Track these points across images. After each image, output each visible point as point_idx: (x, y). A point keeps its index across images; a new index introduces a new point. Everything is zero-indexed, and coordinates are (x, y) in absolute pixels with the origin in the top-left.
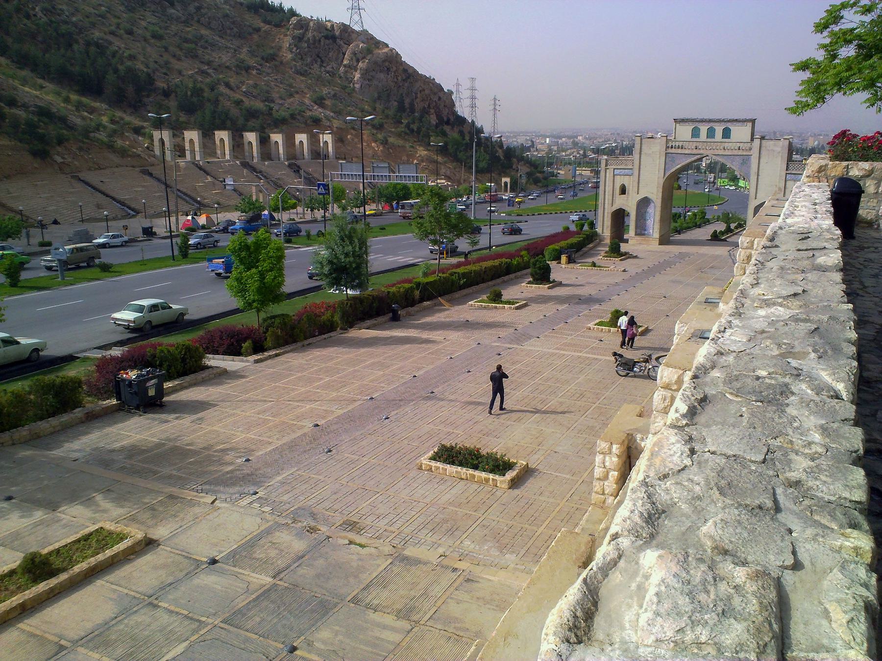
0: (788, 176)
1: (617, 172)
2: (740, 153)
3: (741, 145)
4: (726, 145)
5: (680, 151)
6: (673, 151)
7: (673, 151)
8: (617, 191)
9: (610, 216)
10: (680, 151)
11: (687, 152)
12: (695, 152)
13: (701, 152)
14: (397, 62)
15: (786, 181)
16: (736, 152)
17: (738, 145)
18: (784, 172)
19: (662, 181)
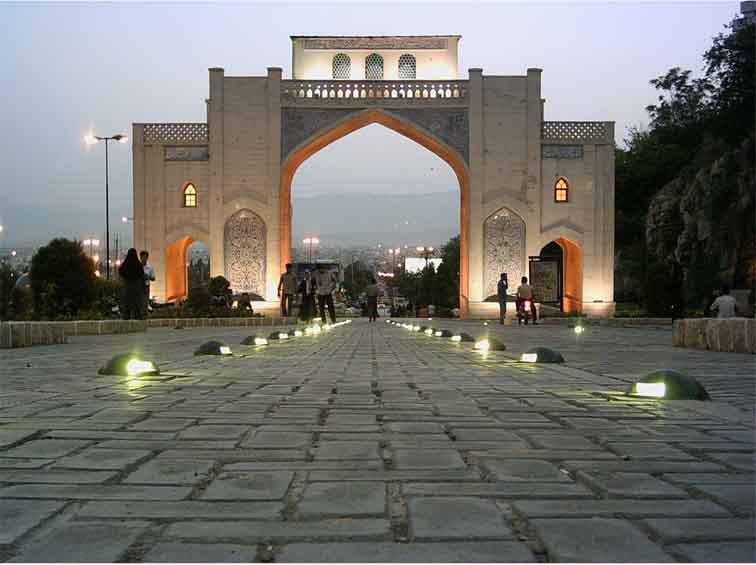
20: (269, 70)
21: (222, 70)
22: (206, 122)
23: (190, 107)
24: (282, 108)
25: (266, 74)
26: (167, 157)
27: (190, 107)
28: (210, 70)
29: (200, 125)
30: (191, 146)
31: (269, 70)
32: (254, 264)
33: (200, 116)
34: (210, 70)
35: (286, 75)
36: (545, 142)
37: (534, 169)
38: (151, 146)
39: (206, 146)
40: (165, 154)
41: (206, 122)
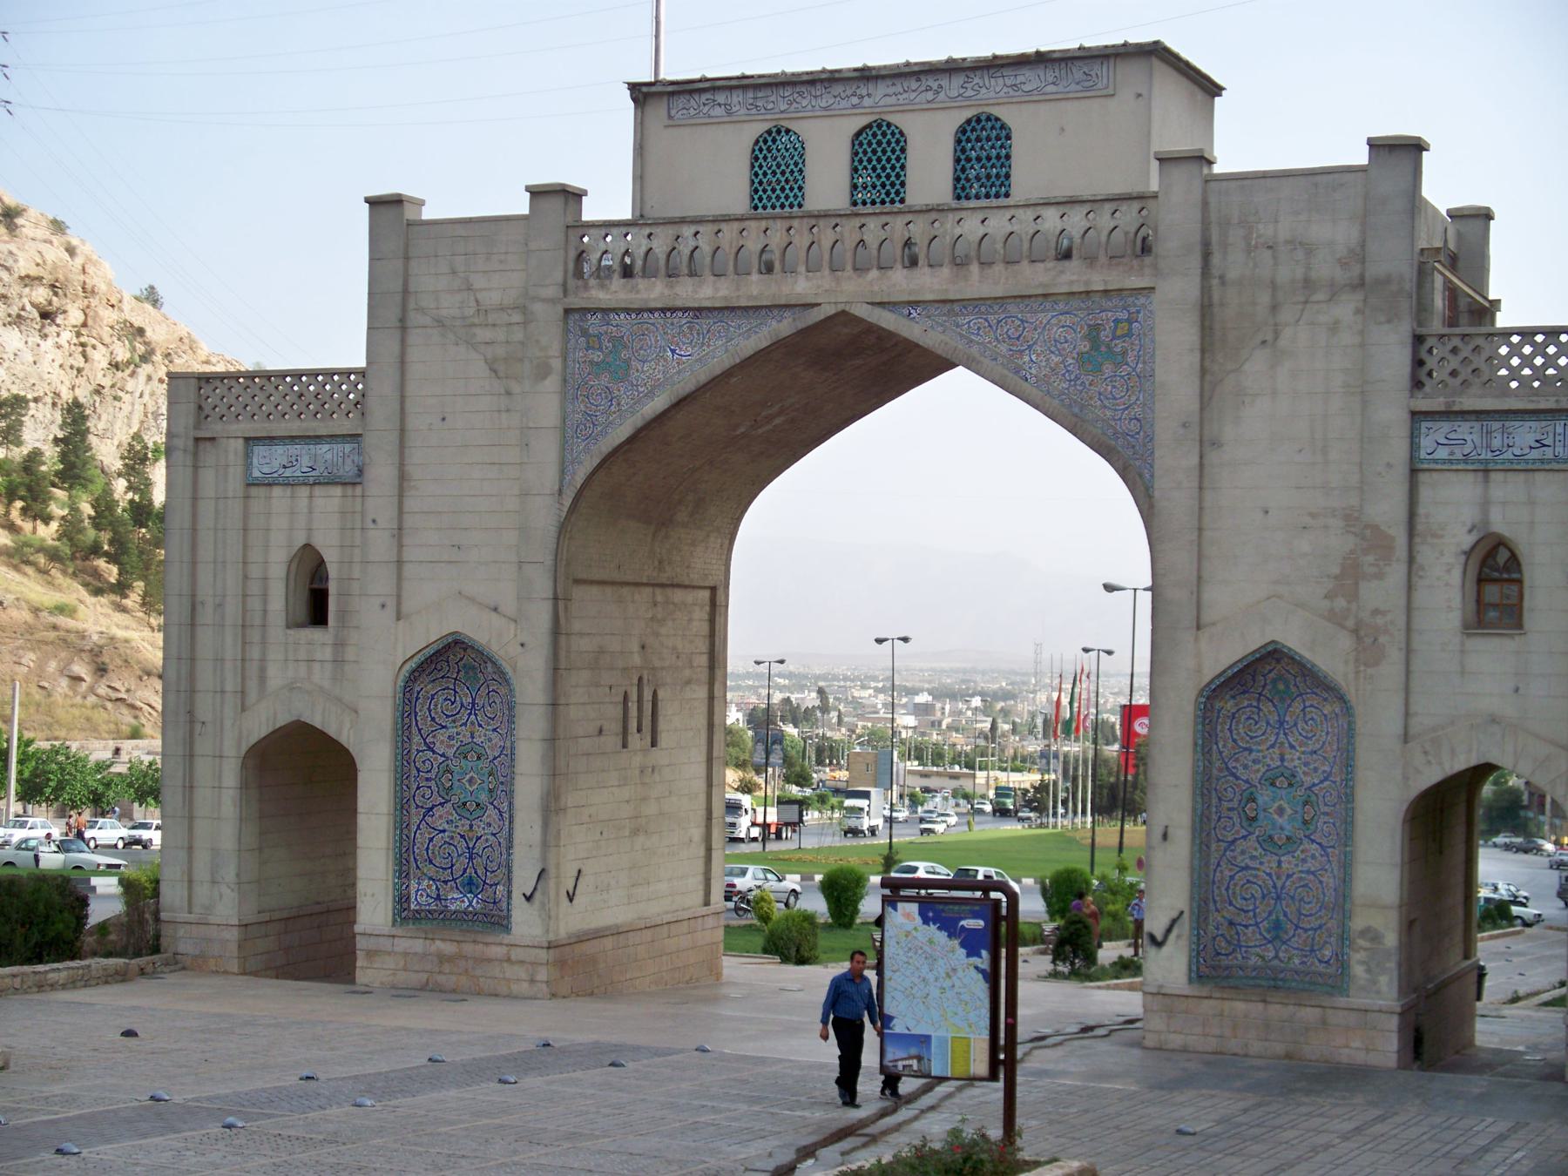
0: (1432, 437)
1: (269, 460)
2: (1072, 276)
3: (1076, 221)
4: (971, 227)
5: (653, 291)
6: (616, 292)
7: (616, 292)
8: (278, 599)
9: (231, 775)
10: (653, 291)
11: (707, 292)
12: (756, 288)
13: (801, 287)
14: (89, 292)
15: (1414, 471)
16: (1036, 277)
17: (1051, 220)
18: (1392, 411)
19: (545, 515)
20: (536, 193)
21: (396, 201)
22: (361, 362)
23: (317, 321)
24: (567, 311)
25: (522, 206)
26: (256, 474)
27: (317, 321)
28: (367, 200)
29: (346, 373)
30: (317, 439)
31: (536, 193)
32: (491, 811)
33: (346, 346)
34: (367, 200)
35: (610, 200)
36: (1423, 404)
37: (1387, 509)
38: (213, 439)
39: (354, 437)
40: (248, 466)
41: (363, 364)
